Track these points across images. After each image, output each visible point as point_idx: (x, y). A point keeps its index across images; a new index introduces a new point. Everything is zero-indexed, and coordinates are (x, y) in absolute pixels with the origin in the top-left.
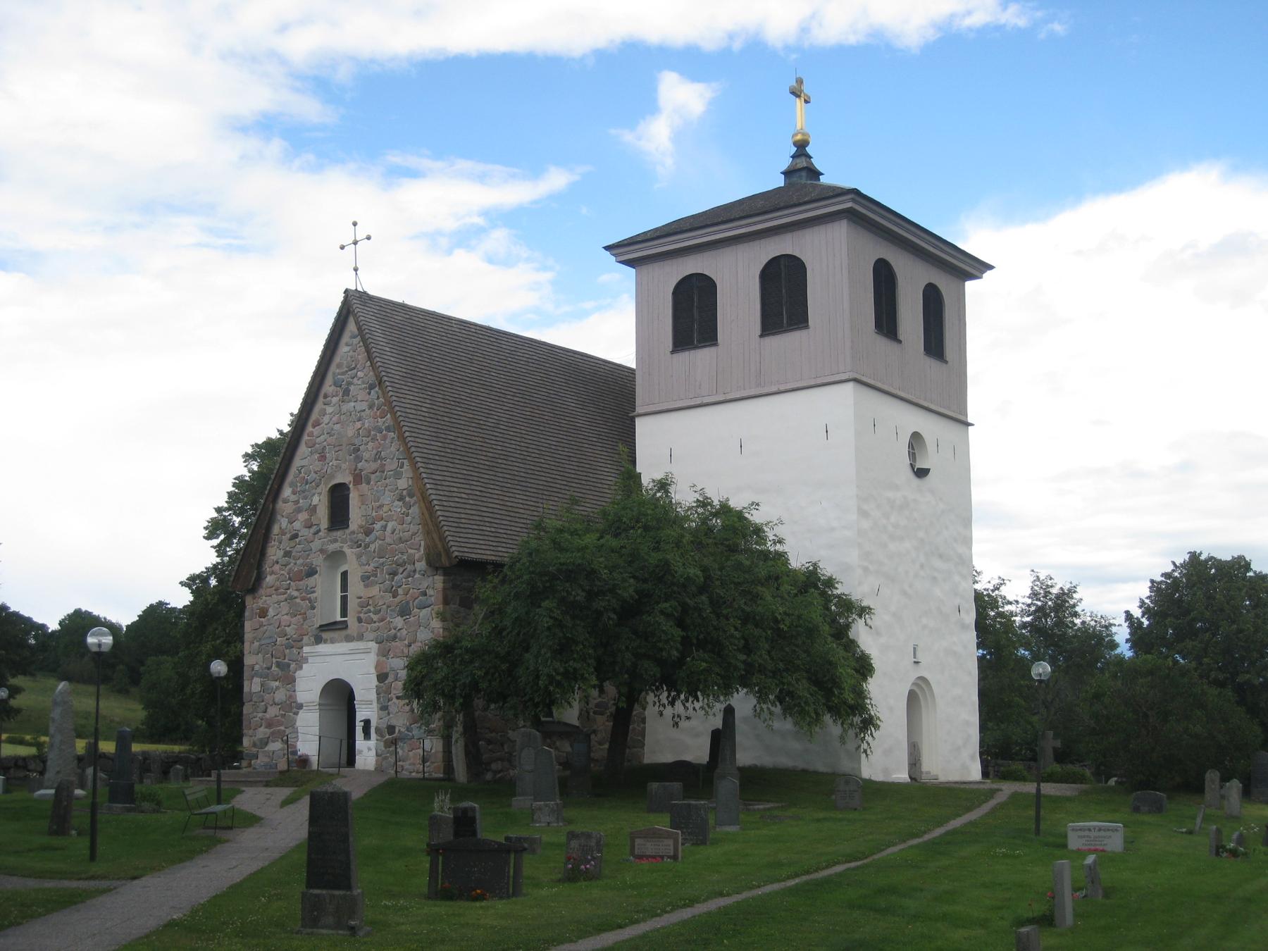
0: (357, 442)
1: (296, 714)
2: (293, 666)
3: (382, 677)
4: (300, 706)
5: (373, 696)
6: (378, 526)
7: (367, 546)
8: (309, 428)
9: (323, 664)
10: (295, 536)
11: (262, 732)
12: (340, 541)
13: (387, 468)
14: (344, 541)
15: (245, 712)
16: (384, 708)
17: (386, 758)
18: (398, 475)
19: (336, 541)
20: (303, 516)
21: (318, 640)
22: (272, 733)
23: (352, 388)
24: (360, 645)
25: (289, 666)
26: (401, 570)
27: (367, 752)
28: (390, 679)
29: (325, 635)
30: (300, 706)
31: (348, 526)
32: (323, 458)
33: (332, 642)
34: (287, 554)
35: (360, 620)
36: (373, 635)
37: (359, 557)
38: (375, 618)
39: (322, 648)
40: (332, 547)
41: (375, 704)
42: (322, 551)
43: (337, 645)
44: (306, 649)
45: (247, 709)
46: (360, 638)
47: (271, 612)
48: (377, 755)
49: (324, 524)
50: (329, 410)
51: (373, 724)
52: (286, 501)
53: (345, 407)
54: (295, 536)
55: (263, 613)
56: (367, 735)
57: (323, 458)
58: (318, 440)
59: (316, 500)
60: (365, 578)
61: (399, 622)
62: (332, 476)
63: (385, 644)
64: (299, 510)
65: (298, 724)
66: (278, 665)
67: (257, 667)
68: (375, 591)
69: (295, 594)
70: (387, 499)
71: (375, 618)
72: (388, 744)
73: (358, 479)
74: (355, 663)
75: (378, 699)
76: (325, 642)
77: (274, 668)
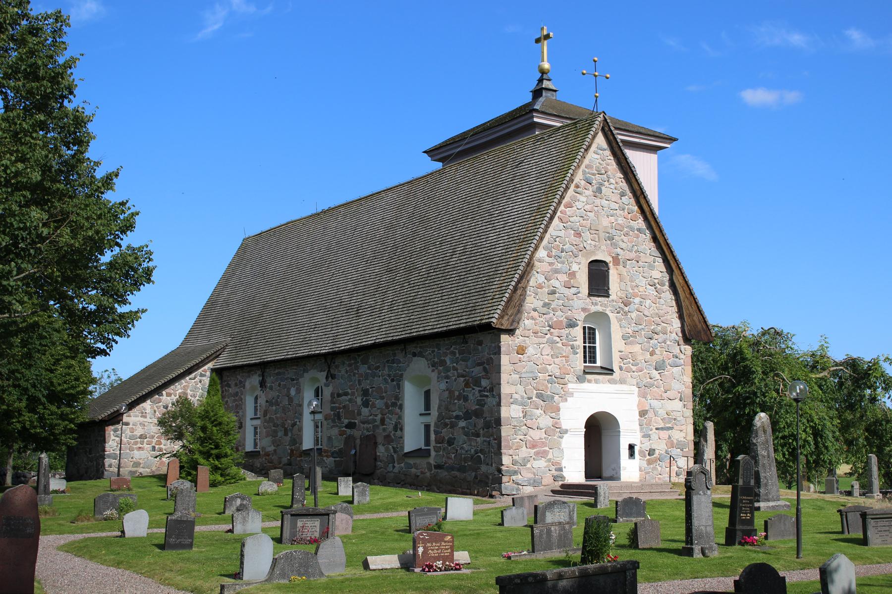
0: (610, 231)
1: (561, 438)
2: (556, 397)
3: (643, 413)
4: (566, 431)
5: (637, 427)
6: (637, 300)
7: (626, 313)
8: (562, 208)
9: (584, 400)
10: (553, 293)
11: (524, 452)
12: (598, 304)
13: (643, 259)
14: (606, 306)
15: (503, 434)
16: (647, 436)
17: (648, 473)
18: (651, 267)
19: (596, 304)
20: (563, 278)
21: (580, 380)
22: (537, 454)
23: (603, 188)
24: (624, 387)
25: (553, 397)
26: (656, 336)
27: (630, 471)
28: (650, 414)
29: (588, 377)
30: (566, 431)
31: (608, 297)
32: (578, 235)
33: (596, 382)
34: (546, 305)
35: (621, 368)
36: (634, 382)
37: (619, 320)
38: (634, 368)
39: (585, 385)
40: (593, 309)
41: (638, 435)
42: (584, 310)
43: (601, 385)
44: (570, 386)
45: (505, 431)
46: (622, 382)
47: (530, 351)
48: (640, 470)
49: (585, 289)
50: (582, 198)
51: (637, 449)
52: (540, 261)
53: (598, 201)
54: (553, 293)
55: (521, 351)
56: (632, 454)
57: (578, 235)
58: (571, 219)
59: (575, 267)
60: (624, 338)
61: (655, 374)
62: (593, 253)
63: (644, 389)
64: (557, 271)
65: (563, 446)
66: (539, 396)
67: (515, 396)
68: (637, 348)
69: (558, 339)
70: (642, 282)
71: (634, 368)
72: (649, 462)
73: (616, 261)
74: (617, 399)
75: (641, 430)
76: (589, 381)
77: (534, 398)
